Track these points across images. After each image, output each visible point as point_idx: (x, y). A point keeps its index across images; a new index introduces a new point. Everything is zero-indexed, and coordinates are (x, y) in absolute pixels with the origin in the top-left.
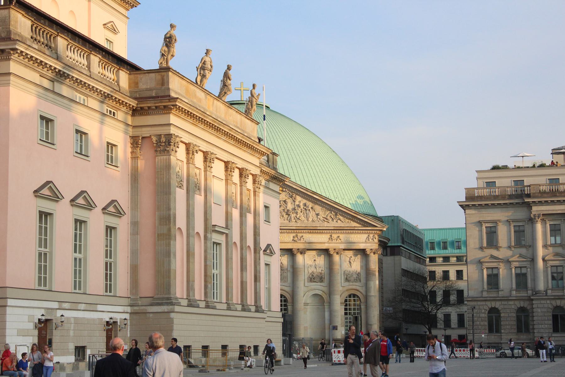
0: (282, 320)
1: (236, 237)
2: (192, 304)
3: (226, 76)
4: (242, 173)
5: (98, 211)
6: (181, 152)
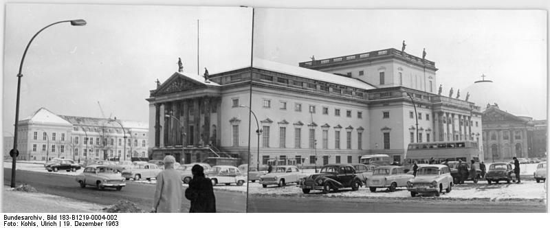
1: (463, 133)
3: (458, 92)
4: (464, 116)
5: (424, 131)
6: (445, 115)
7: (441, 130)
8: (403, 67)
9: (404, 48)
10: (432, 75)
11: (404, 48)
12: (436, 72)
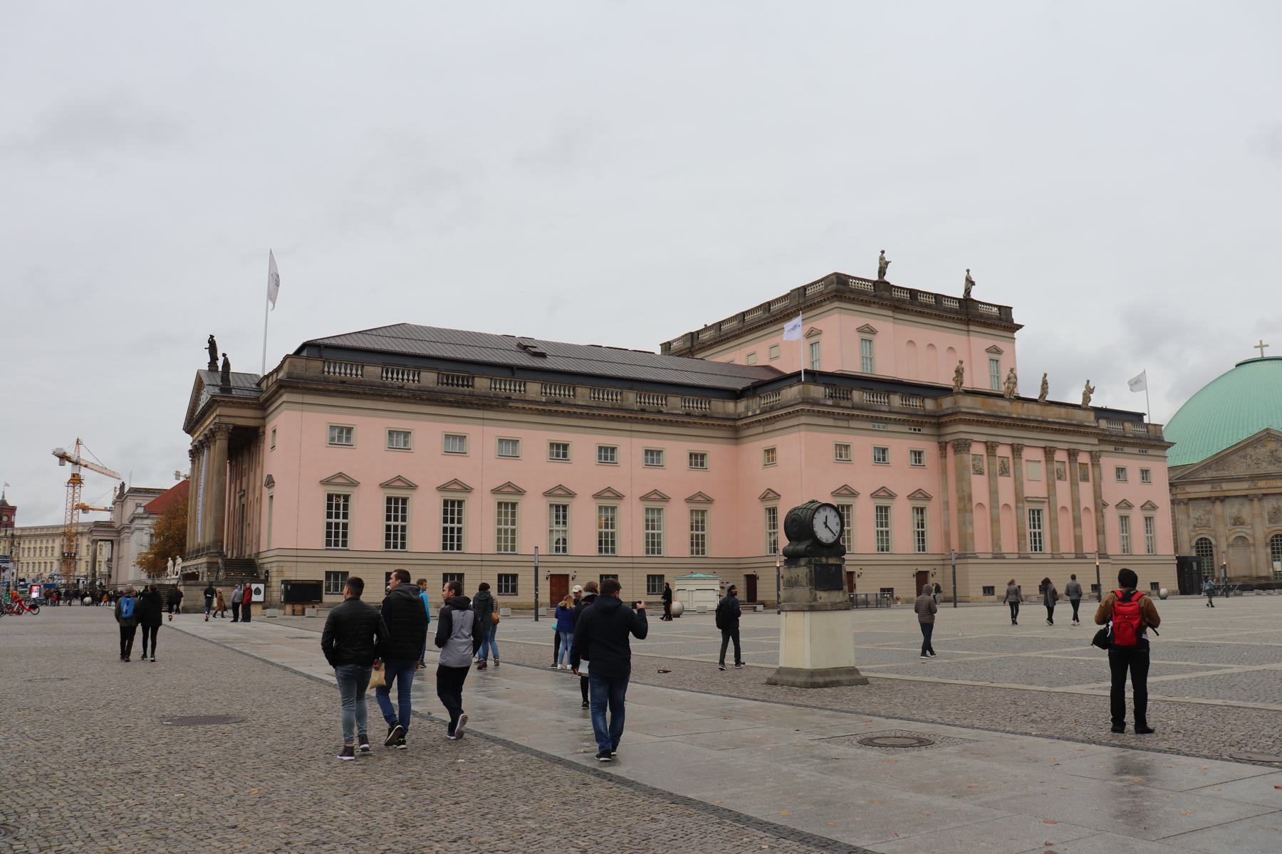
0: (1176, 562)
2: (998, 556)
6: (978, 449)
7: (965, 499)
8: (875, 323)
9: (882, 272)
10: (1001, 344)
11: (882, 272)
12: (1017, 334)
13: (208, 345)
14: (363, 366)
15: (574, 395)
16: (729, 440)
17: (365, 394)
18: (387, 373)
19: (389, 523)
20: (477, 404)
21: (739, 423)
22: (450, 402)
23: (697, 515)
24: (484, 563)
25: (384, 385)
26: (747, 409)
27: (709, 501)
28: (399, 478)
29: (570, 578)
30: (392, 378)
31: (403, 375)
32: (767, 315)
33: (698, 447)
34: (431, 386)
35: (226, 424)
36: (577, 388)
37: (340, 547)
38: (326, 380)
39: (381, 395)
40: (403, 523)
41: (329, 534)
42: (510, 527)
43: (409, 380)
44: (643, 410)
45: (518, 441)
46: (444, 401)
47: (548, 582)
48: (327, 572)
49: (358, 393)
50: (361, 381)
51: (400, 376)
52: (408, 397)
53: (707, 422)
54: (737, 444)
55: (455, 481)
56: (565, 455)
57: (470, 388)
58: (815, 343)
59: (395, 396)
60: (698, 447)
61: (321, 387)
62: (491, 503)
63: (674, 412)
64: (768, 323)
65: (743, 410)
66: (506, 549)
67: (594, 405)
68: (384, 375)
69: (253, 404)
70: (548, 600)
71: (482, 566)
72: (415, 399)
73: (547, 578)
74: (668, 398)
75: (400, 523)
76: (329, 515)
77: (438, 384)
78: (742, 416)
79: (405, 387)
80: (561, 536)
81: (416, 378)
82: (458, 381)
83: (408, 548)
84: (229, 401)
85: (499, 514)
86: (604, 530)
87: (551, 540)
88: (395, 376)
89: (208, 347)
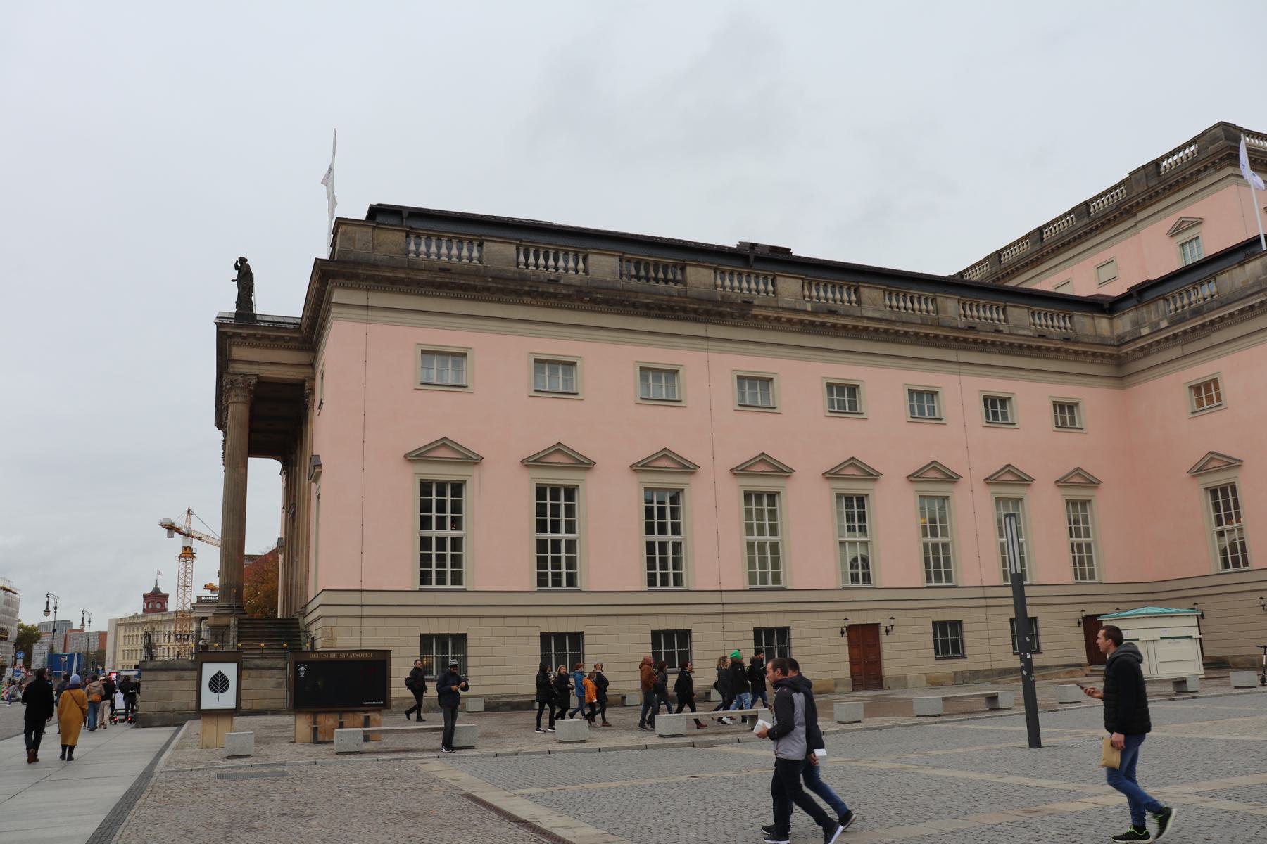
13: (235, 274)
14: (480, 245)
15: (859, 302)
16: (1105, 381)
17: (488, 289)
18: (527, 257)
19: (542, 536)
20: (695, 311)
21: (1127, 349)
22: (647, 306)
23: (1075, 510)
24: (728, 609)
25: (523, 279)
26: (1137, 324)
27: (1093, 483)
28: (559, 448)
29: (883, 630)
30: (537, 266)
31: (556, 260)
32: (1086, 220)
33: (1066, 391)
34: (609, 279)
35: (245, 375)
36: (862, 289)
37: (449, 585)
38: (412, 266)
39: (516, 292)
40: (570, 536)
41: (425, 561)
42: (768, 538)
43: (568, 268)
44: (972, 328)
45: (771, 379)
46: (634, 305)
47: (845, 640)
48: (423, 637)
49: (474, 288)
50: (478, 269)
51: (551, 262)
52: (567, 297)
53: (1076, 348)
54: (1123, 388)
55: (665, 454)
56: (853, 405)
57: (680, 286)
58: (1189, 242)
59: (542, 295)
60: (1066, 391)
61: (402, 275)
62: (732, 493)
63: (1021, 332)
64: (1091, 230)
65: (1128, 328)
66: (764, 581)
67: (893, 318)
68: (522, 259)
69: (291, 339)
70: (847, 675)
71: (723, 613)
72: (581, 300)
73: (842, 633)
74: (1008, 308)
75: (563, 536)
76: (425, 523)
77: (621, 275)
78: (1128, 339)
79: (562, 282)
80: (859, 552)
81: (581, 265)
82: (656, 272)
83: (581, 583)
84: (249, 335)
85: (748, 513)
86: (930, 540)
87: (843, 560)
88: (542, 261)
89: (236, 278)
